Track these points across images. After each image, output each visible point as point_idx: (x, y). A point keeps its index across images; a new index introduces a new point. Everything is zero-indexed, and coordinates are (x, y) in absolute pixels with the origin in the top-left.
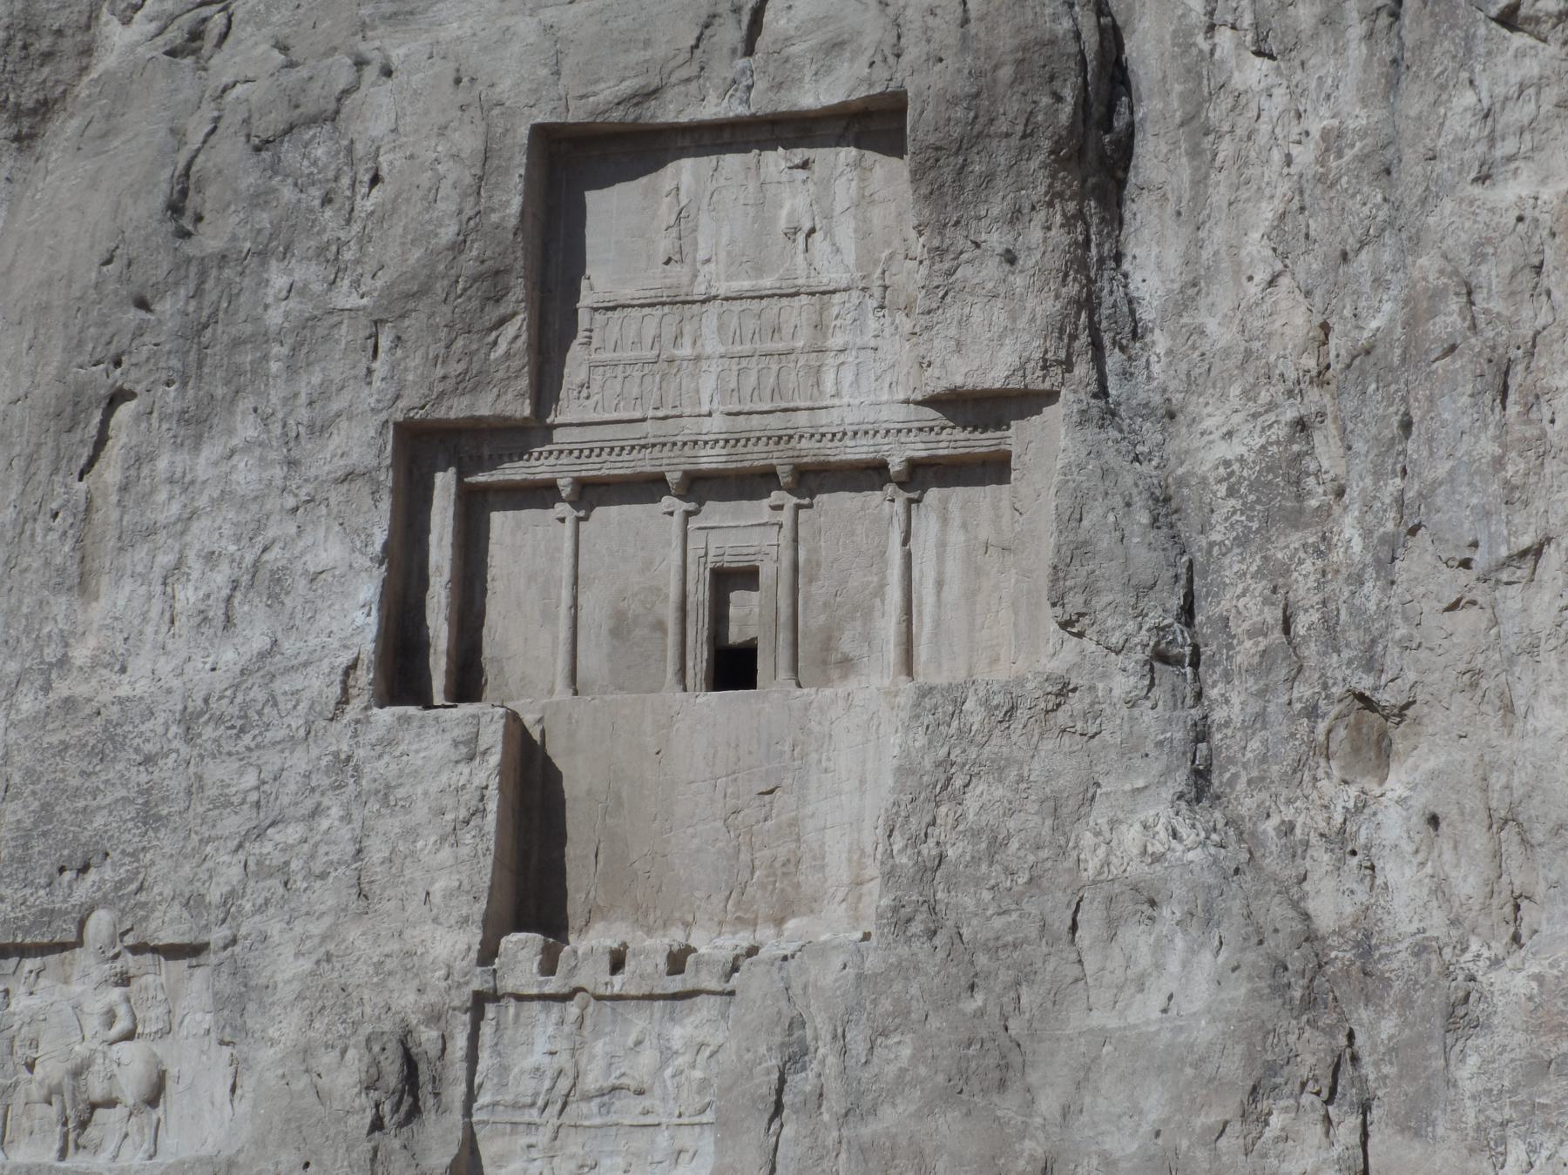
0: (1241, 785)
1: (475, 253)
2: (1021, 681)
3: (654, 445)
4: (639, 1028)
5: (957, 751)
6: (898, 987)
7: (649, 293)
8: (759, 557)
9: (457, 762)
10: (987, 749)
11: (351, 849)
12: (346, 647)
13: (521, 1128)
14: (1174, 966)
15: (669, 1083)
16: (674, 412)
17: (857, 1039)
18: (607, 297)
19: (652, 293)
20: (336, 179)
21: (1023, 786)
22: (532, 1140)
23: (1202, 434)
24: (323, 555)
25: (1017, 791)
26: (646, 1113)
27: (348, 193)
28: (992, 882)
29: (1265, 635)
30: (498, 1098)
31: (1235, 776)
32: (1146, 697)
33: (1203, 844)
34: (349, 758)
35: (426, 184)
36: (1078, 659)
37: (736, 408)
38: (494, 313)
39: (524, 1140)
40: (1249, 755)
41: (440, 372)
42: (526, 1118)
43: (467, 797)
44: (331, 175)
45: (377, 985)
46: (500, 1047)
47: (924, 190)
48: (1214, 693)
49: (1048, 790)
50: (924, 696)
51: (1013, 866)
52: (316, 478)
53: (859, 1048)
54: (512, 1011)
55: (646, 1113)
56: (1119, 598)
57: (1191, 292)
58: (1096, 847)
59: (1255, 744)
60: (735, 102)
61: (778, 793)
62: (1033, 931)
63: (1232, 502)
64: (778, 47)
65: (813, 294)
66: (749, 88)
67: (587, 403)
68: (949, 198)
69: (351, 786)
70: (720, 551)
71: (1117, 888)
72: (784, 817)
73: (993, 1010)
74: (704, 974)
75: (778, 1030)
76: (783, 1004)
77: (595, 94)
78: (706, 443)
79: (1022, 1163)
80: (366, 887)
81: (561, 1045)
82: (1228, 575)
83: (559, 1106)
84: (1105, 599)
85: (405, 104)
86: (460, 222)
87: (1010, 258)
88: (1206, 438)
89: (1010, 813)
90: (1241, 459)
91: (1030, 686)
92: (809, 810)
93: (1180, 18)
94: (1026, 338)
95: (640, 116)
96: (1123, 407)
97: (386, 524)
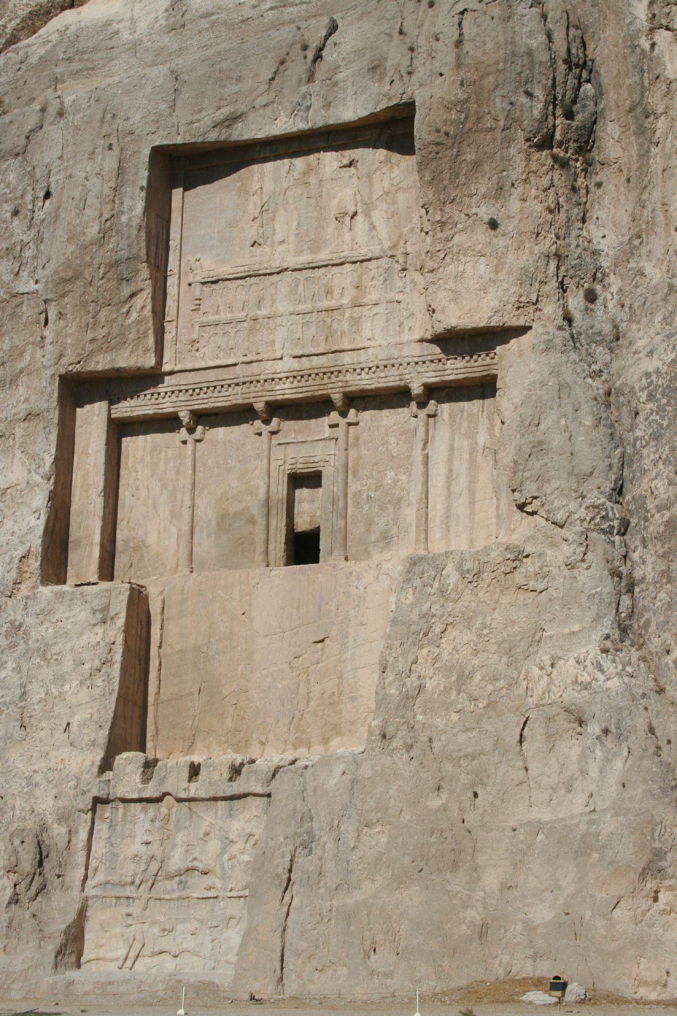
0: (652, 628)
1: (111, 246)
2: (486, 551)
3: (244, 383)
4: (208, 823)
5: (437, 606)
6: (380, 788)
7: (242, 269)
8: (321, 464)
9: (94, 625)
10: (460, 604)
11: (18, 692)
12: (22, 542)
13: (122, 901)
14: (593, 772)
15: (226, 865)
16: (259, 357)
17: (348, 828)
18: (212, 274)
19: (246, 268)
20: (22, 196)
21: (486, 631)
22: (130, 910)
23: (634, 353)
24: (10, 475)
25: (479, 636)
26: (210, 888)
27: (30, 207)
28: (460, 706)
29: (668, 509)
30: (109, 878)
31: (648, 622)
32: (583, 560)
33: (619, 675)
34: (21, 625)
35: (78, 196)
36: (532, 532)
37: (300, 353)
38: (127, 290)
39: (124, 910)
40: (658, 604)
41: (90, 336)
42: (128, 893)
43: (100, 651)
44: (19, 193)
45: (26, 793)
46: (113, 839)
47: (427, 177)
48: (635, 556)
49: (505, 635)
50: (415, 564)
51: (476, 694)
52: (6, 418)
53: (350, 837)
54: (121, 811)
55: (210, 888)
56: (564, 484)
57: (636, 242)
58: (541, 677)
59: (662, 595)
60: (298, 119)
61: (327, 641)
62: (488, 745)
63: (650, 405)
64: (328, 75)
65: (354, 262)
66: (309, 108)
67: (197, 354)
68: (446, 182)
69: (22, 647)
70: (293, 461)
71: (555, 710)
73: (454, 806)
74: (253, 782)
75: (293, 822)
76: (299, 803)
77: (199, 121)
78: (280, 379)
79: (463, 927)
80: (27, 720)
81: (155, 837)
82: (647, 463)
83: (149, 884)
84: (554, 485)
85: (69, 137)
86: (100, 222)
87: (493, 225)
88: (637, 356)
89: (476, 652)
90: (658, 372)
91: (493, 554)
92: (348, 655)
93: (628, 25)
94: (505, 286)
95: (230, 134)
96: (583, 336)
97: (53, 450)
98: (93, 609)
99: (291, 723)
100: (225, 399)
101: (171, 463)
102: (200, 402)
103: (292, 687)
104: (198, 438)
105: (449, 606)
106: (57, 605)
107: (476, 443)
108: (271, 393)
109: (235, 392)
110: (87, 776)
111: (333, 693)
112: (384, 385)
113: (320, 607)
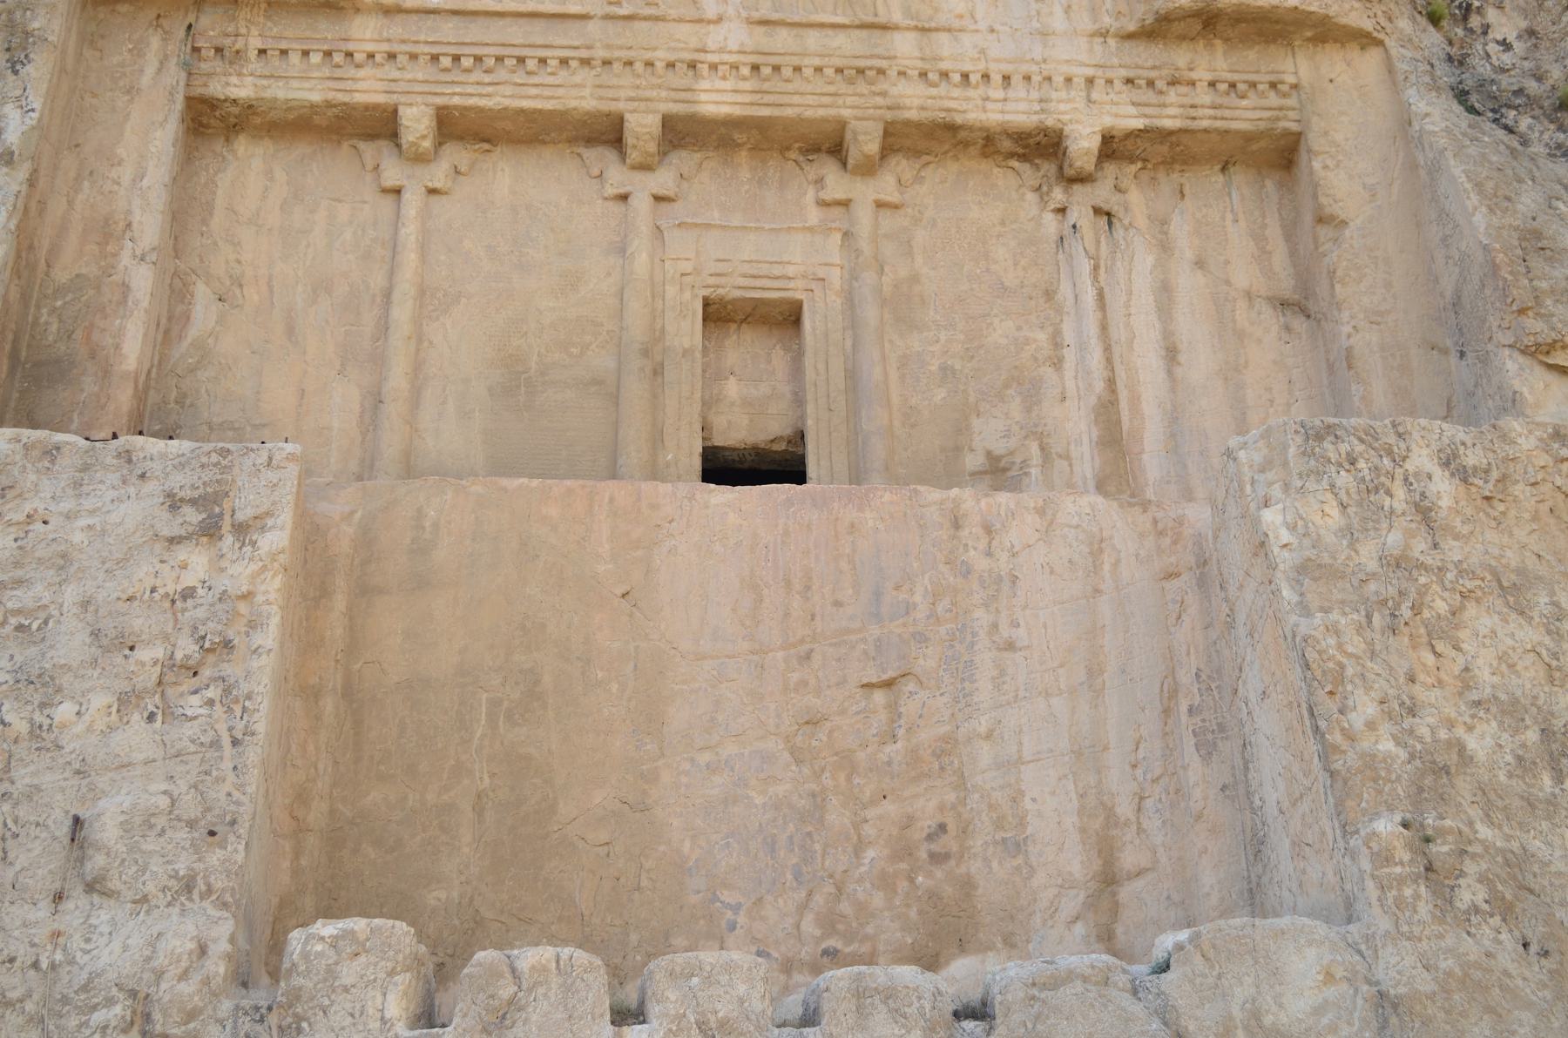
3: (607, 63)
8: (800, 284)
9: (173, 541)
37: (775, 16)
43: (200, 613)
50: (1319, 438)
70: (721, 267)
72: (925, 736)
98: (170, 495)
99: (803, 908)
100: (547, 92)
101: (348, 236)
102: (470, 89)
103: (802, 803)
104: (438, 185)
105: (1454, 551)
106: (33, 477)
107: (1228, 282)
108: (683, 95)
109: (577, 79)
110: (186, 988)
111: (942, 828)
112: (998, 117)
113: (878, 595)
